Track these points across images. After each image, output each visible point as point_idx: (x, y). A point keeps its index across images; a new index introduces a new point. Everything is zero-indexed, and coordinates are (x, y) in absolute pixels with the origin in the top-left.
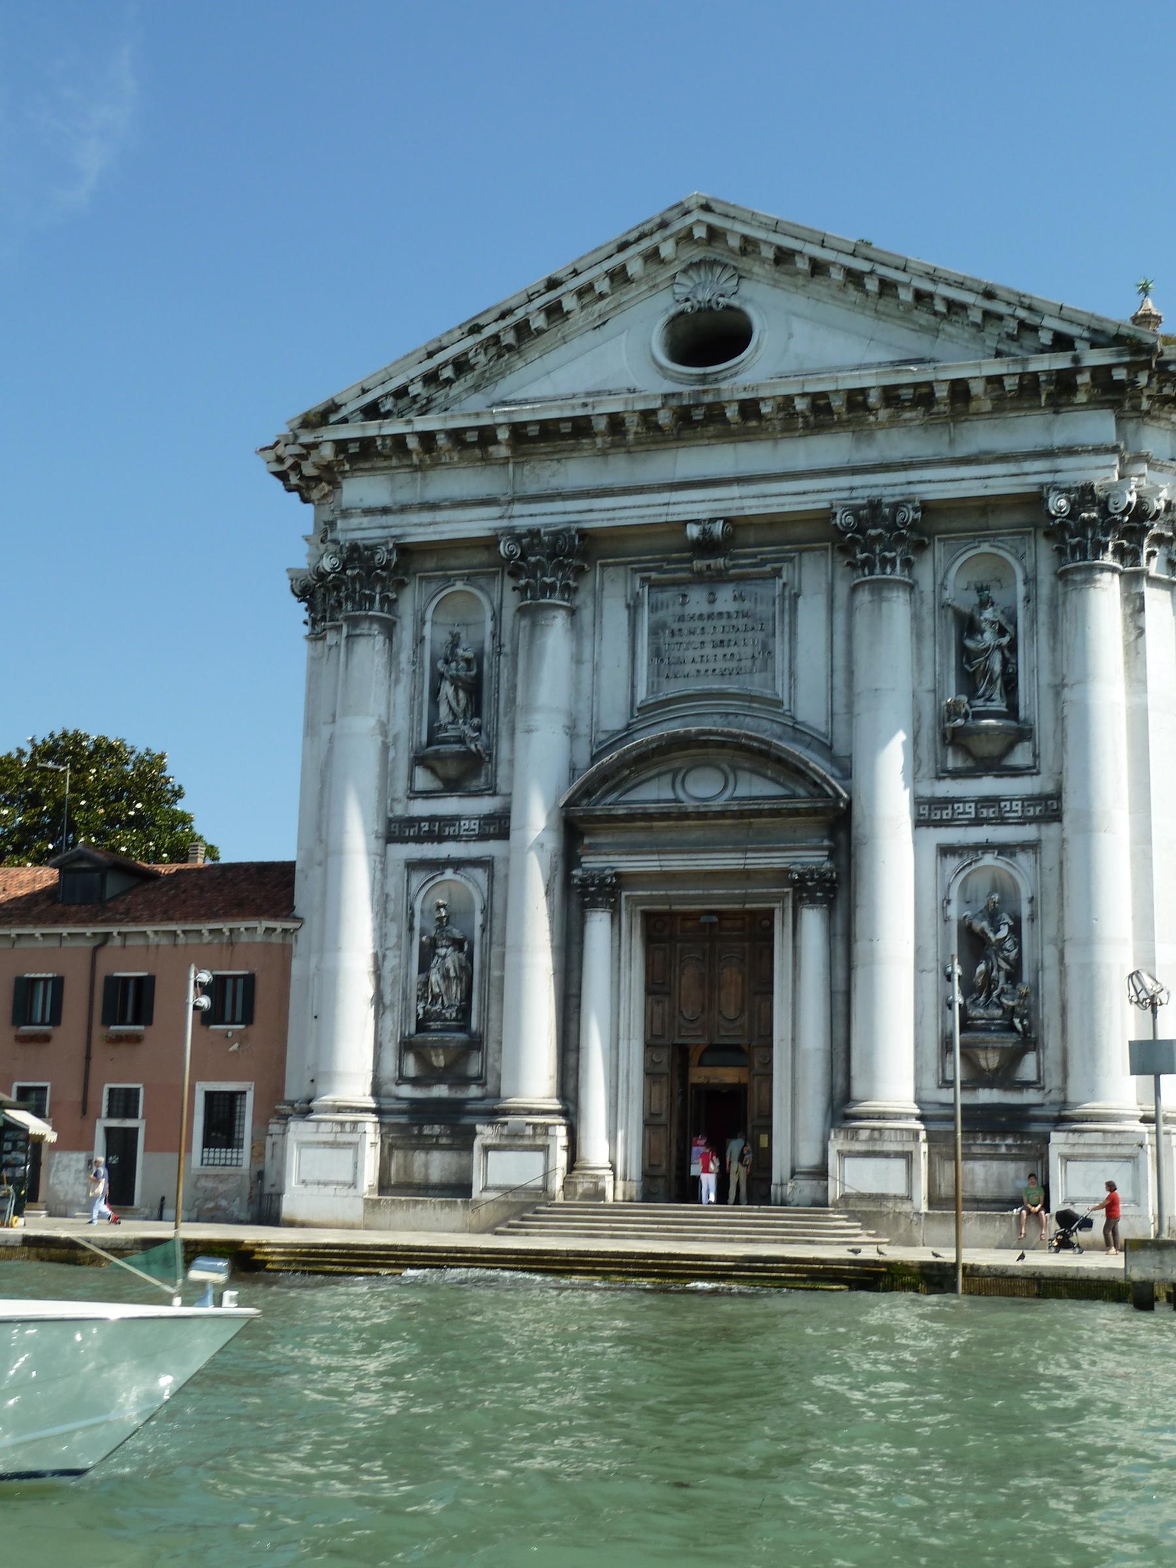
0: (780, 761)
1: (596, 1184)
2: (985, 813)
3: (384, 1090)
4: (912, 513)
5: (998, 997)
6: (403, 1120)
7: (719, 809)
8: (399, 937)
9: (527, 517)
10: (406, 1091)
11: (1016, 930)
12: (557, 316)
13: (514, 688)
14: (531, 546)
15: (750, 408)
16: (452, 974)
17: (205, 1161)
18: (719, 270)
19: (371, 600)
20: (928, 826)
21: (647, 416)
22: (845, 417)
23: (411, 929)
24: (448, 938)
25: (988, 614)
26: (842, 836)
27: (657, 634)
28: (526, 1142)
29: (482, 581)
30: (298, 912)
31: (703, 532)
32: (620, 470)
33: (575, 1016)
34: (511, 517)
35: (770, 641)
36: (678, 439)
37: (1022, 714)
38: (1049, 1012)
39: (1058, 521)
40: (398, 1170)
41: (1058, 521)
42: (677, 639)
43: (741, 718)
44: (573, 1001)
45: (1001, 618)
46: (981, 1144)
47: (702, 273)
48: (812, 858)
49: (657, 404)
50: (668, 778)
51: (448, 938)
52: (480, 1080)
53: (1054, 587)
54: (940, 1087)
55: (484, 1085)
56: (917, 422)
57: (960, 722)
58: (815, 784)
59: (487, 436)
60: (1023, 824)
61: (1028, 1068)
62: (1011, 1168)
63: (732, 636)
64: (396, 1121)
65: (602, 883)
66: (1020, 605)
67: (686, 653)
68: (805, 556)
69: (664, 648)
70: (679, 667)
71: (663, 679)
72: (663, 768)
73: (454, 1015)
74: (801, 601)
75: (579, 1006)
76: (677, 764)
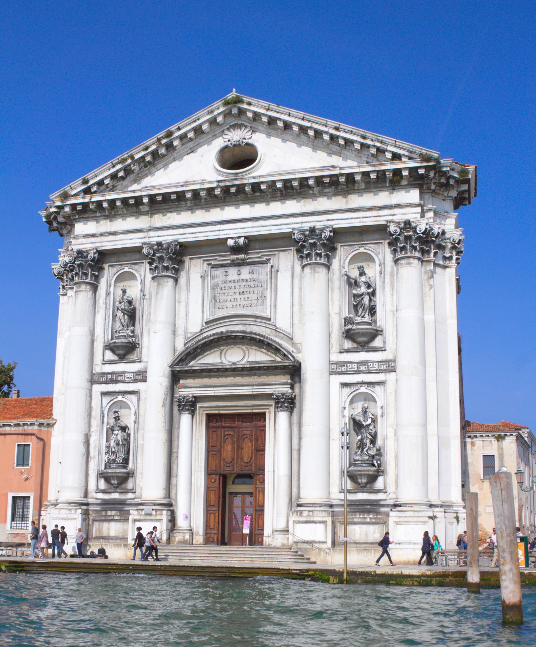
0: (269, 345)
1: (184, 537)
2: (362, 368)
3: (90, 495)
4: (329, 233)
5: (367, 451)
6: (98, 508)
7: (241, 366)
8: (97, 426)
10: (101, 496)
11: (374, 421)
12: (171, 148)
13: (150, 314)
14: (158, 250)
15: (256, 187)
16: (121, 443)
17: (13, 527)
18: (243, 128)
19: (86, 274)
20: (336, 374)
21: (210, 191)
22: (299, 191)
23: (103, 423)
24: (119, 426)
25: (363, 279)
26: (297, 379)
27: (214, 289)
28: (152, 518)
29: (136, 267)
30: (54, 417)
31: (236, 242)
33: (176, 461)
34: (149, 237)
35: (265, 291)
36: (224, 202)
37: (378, 324)
39: (394, 237)
40: (96, 531)
41: (394, 237)
42: (224, 291)
43: (251, 326)
44: (174, 455)
45: (368, 281)
46: (358, 517)
47: (236, 130)
49: (215, 185)
50: (219, 352)
51: (119, 426)
52: (133, 491)
53: (392, 268)
54: (340, 492)
55: (135, 492)
56: (331, 193)
57: (350, 327)
58: (285, 355)
59: (138, 200)
60: (379, 373)
61: (379, 484)
62: (372, 528)
63: (248, 290)
64: (95, 509)
65: (188, 401)
66: (378, 275)
67: (227, 297)
68: (281, 253)
69: (217, 295)
70: (224, 304)
71: (217, 309)
72: (217, 349)
73: (121, 461)
74: (279, 273)
75: (177, 457)
76: (222, 348)
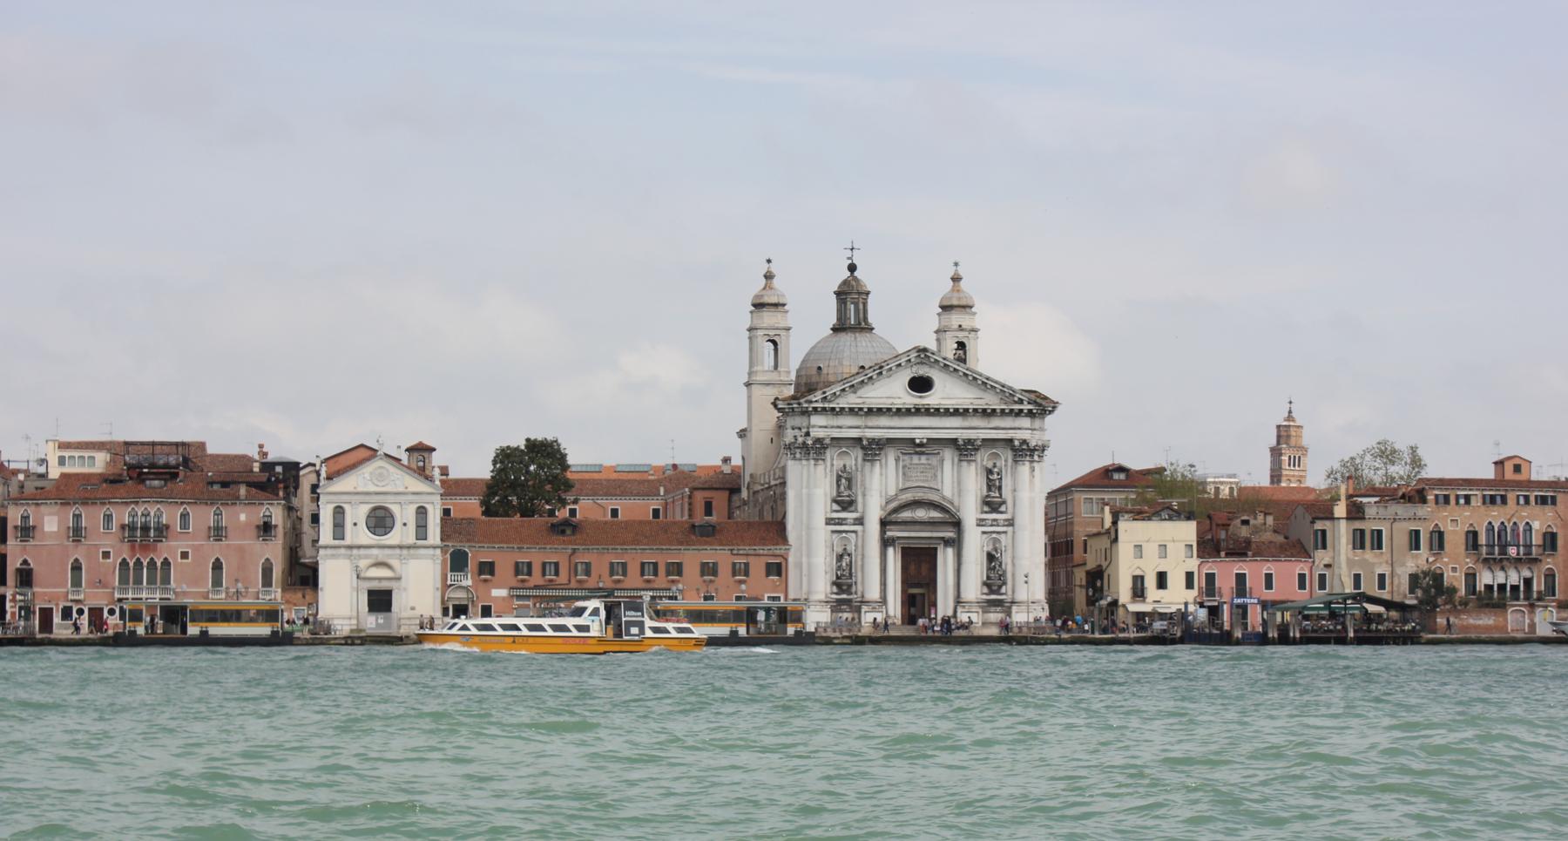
9: (870, 434)
32: (896, 422)
38: (1009, 575)
48: (950, 534)
